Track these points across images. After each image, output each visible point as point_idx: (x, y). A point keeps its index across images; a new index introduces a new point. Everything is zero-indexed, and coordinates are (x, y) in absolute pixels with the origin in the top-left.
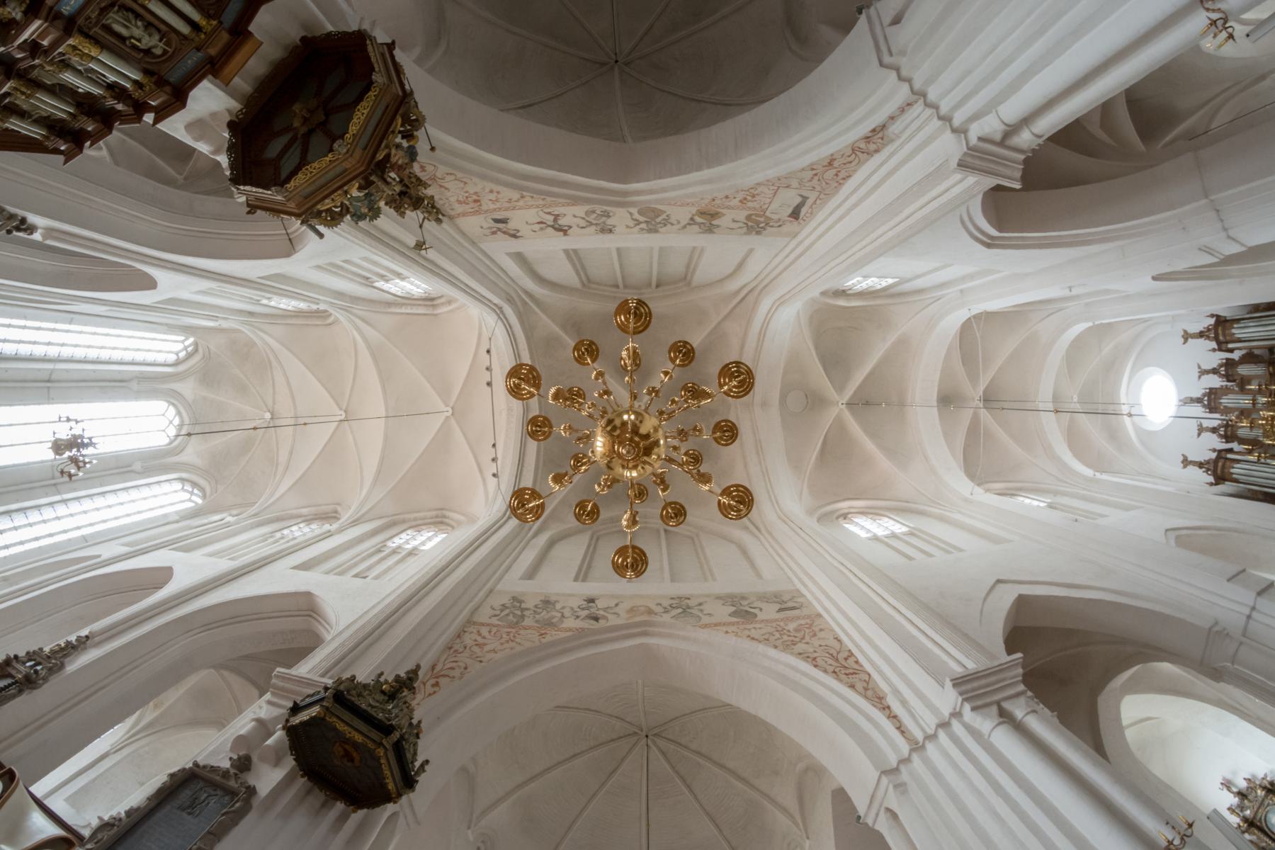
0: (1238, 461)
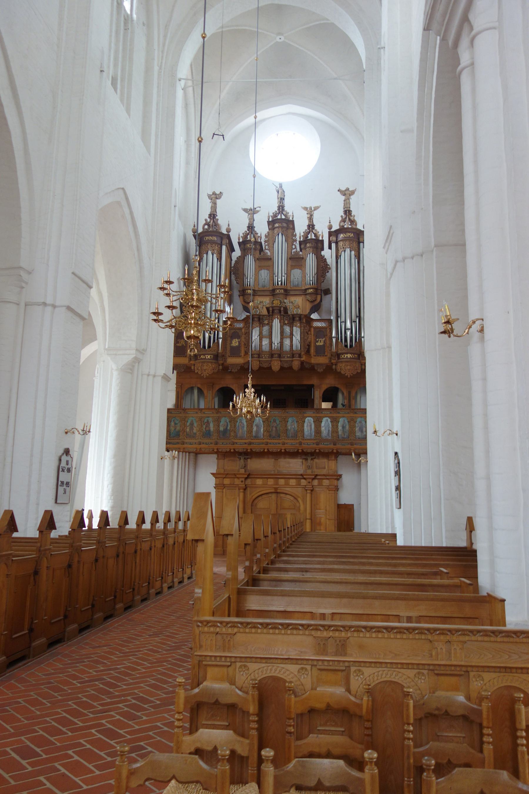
0: (220, 259)
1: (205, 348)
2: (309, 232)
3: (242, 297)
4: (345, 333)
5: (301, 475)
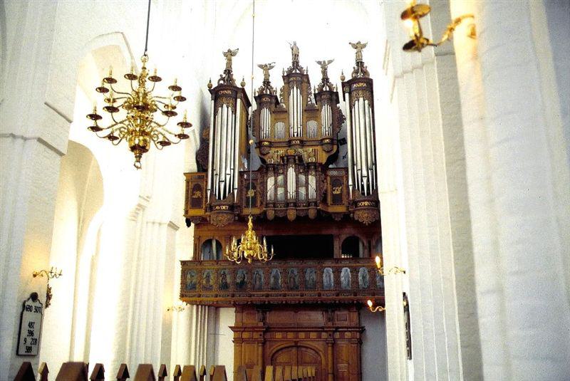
0: (234, 112)
2: (324, 86)
3: (258, 150)
4: (362, 181)
5: (322, 328)
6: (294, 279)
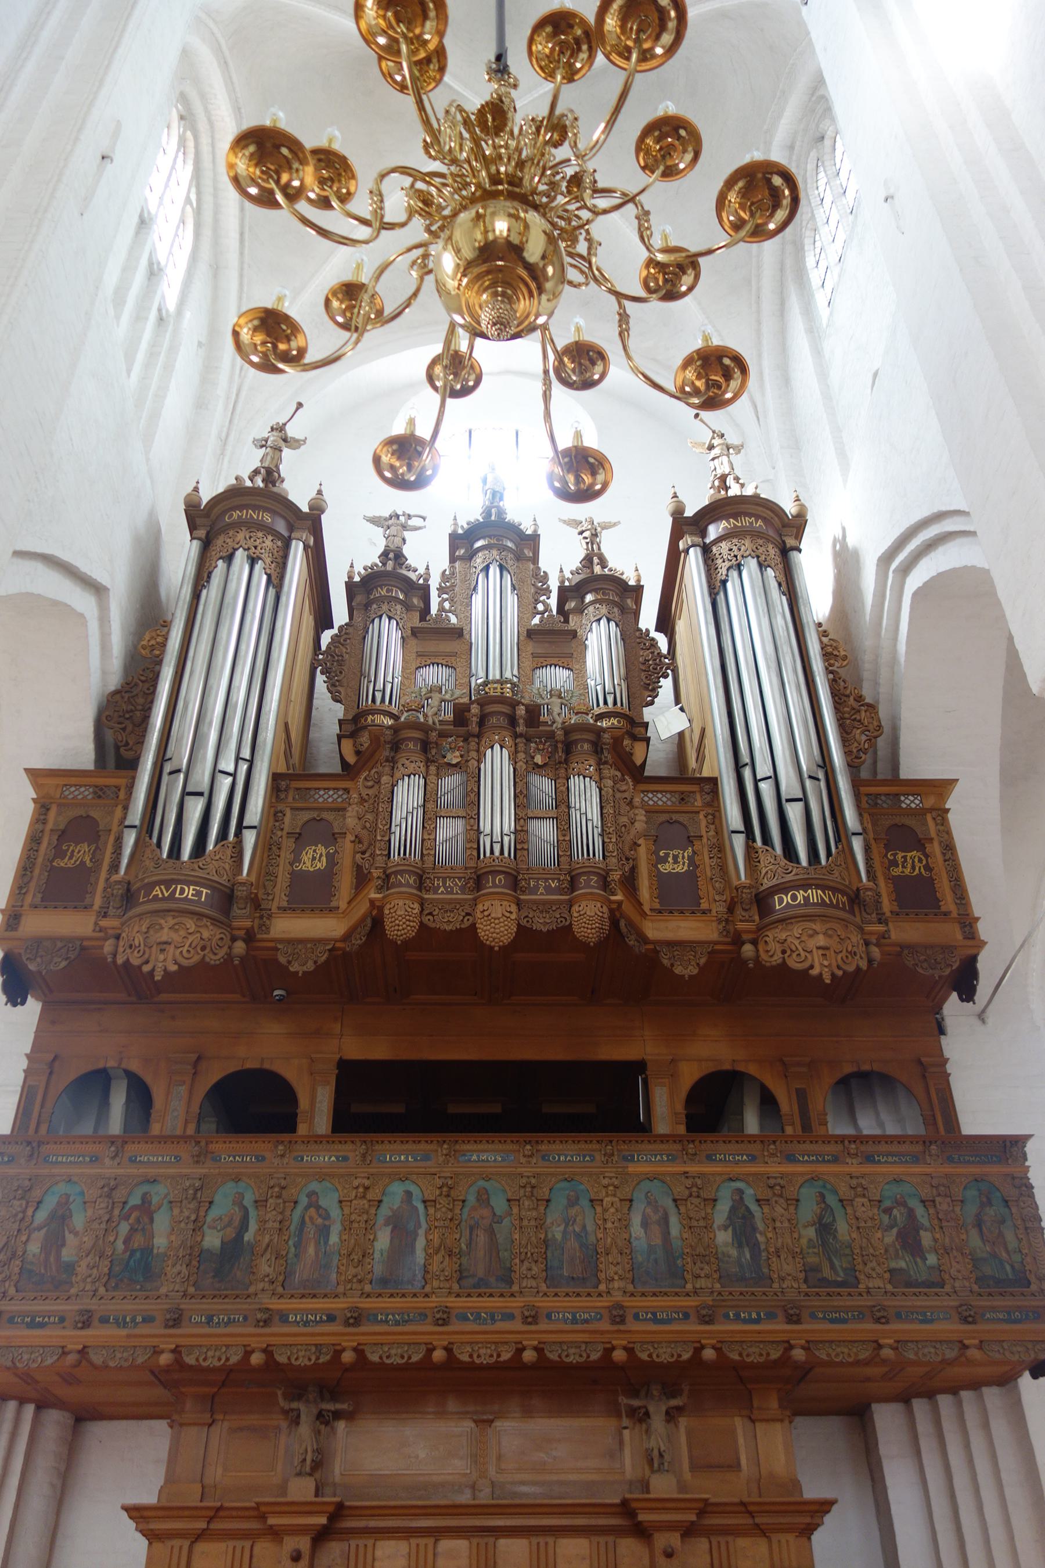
1: (178, 856)
6: (491, 1233)
